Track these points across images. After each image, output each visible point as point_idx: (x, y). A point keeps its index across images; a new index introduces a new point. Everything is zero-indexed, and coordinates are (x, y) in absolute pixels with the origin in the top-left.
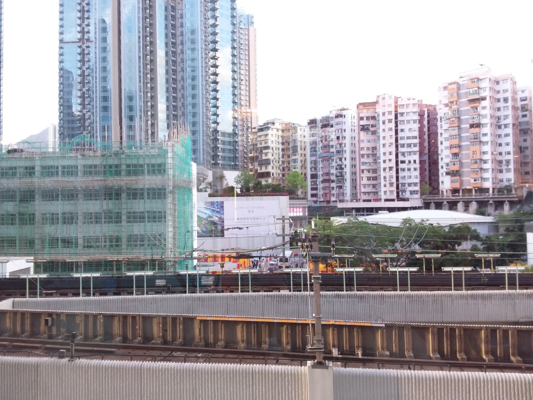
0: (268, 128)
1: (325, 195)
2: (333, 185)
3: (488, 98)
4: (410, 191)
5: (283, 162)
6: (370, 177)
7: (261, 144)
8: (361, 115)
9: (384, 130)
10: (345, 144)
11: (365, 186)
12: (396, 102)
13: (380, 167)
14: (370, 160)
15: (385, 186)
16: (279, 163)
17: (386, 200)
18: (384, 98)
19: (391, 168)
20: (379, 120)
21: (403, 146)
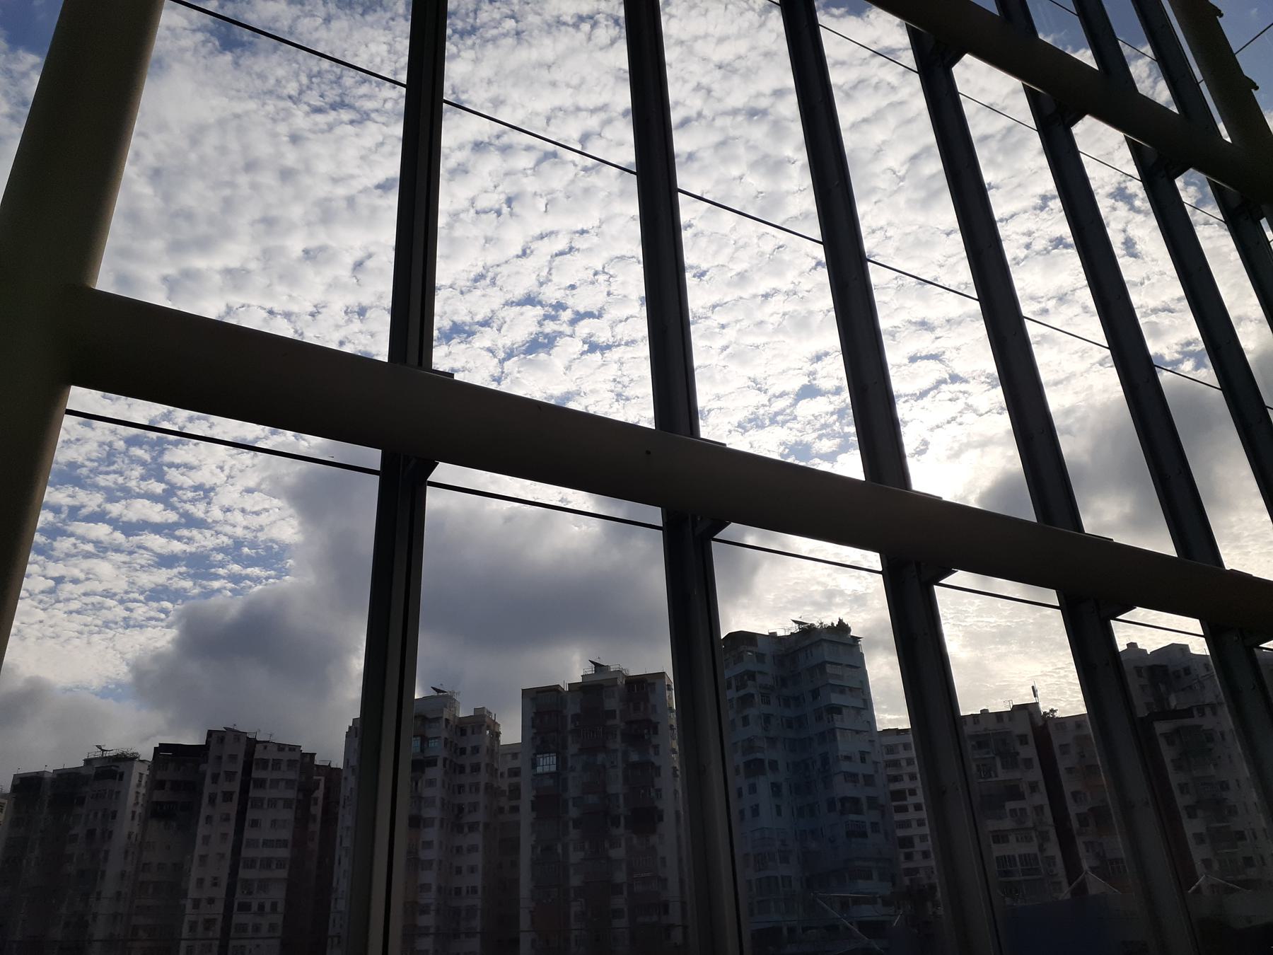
3: (440, 763)
21: (251, 864)
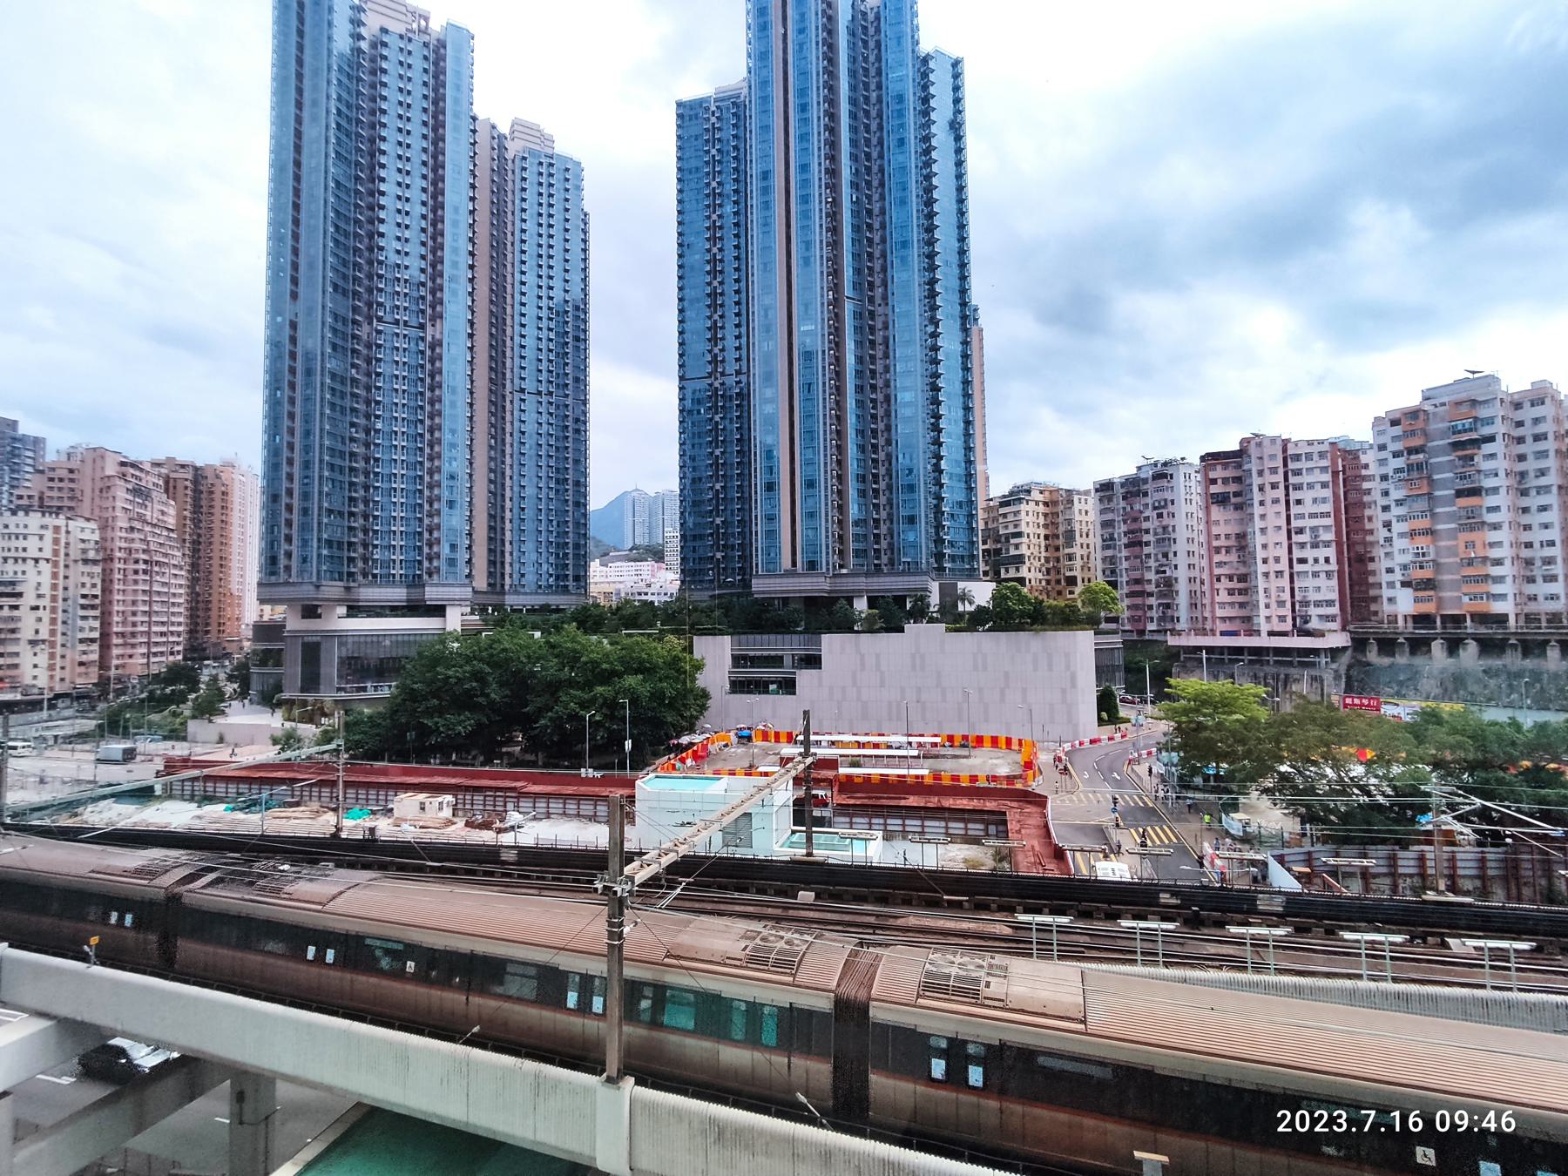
1: (1132, 619)
2: (1152, 601)
4: (1320, 616)
5: (1047, 560)
7: (1006, 527)
8: (1212, 475)
9: (1262, 503)
11: (1222, 605)
12: (1285, 450)
13: (1256, 572)
14: (1233, 557)
15: (1267, 606)
17: (1271, 634)
18: (1259, 445)
19: (1279, 573)
20: (1251, 485)
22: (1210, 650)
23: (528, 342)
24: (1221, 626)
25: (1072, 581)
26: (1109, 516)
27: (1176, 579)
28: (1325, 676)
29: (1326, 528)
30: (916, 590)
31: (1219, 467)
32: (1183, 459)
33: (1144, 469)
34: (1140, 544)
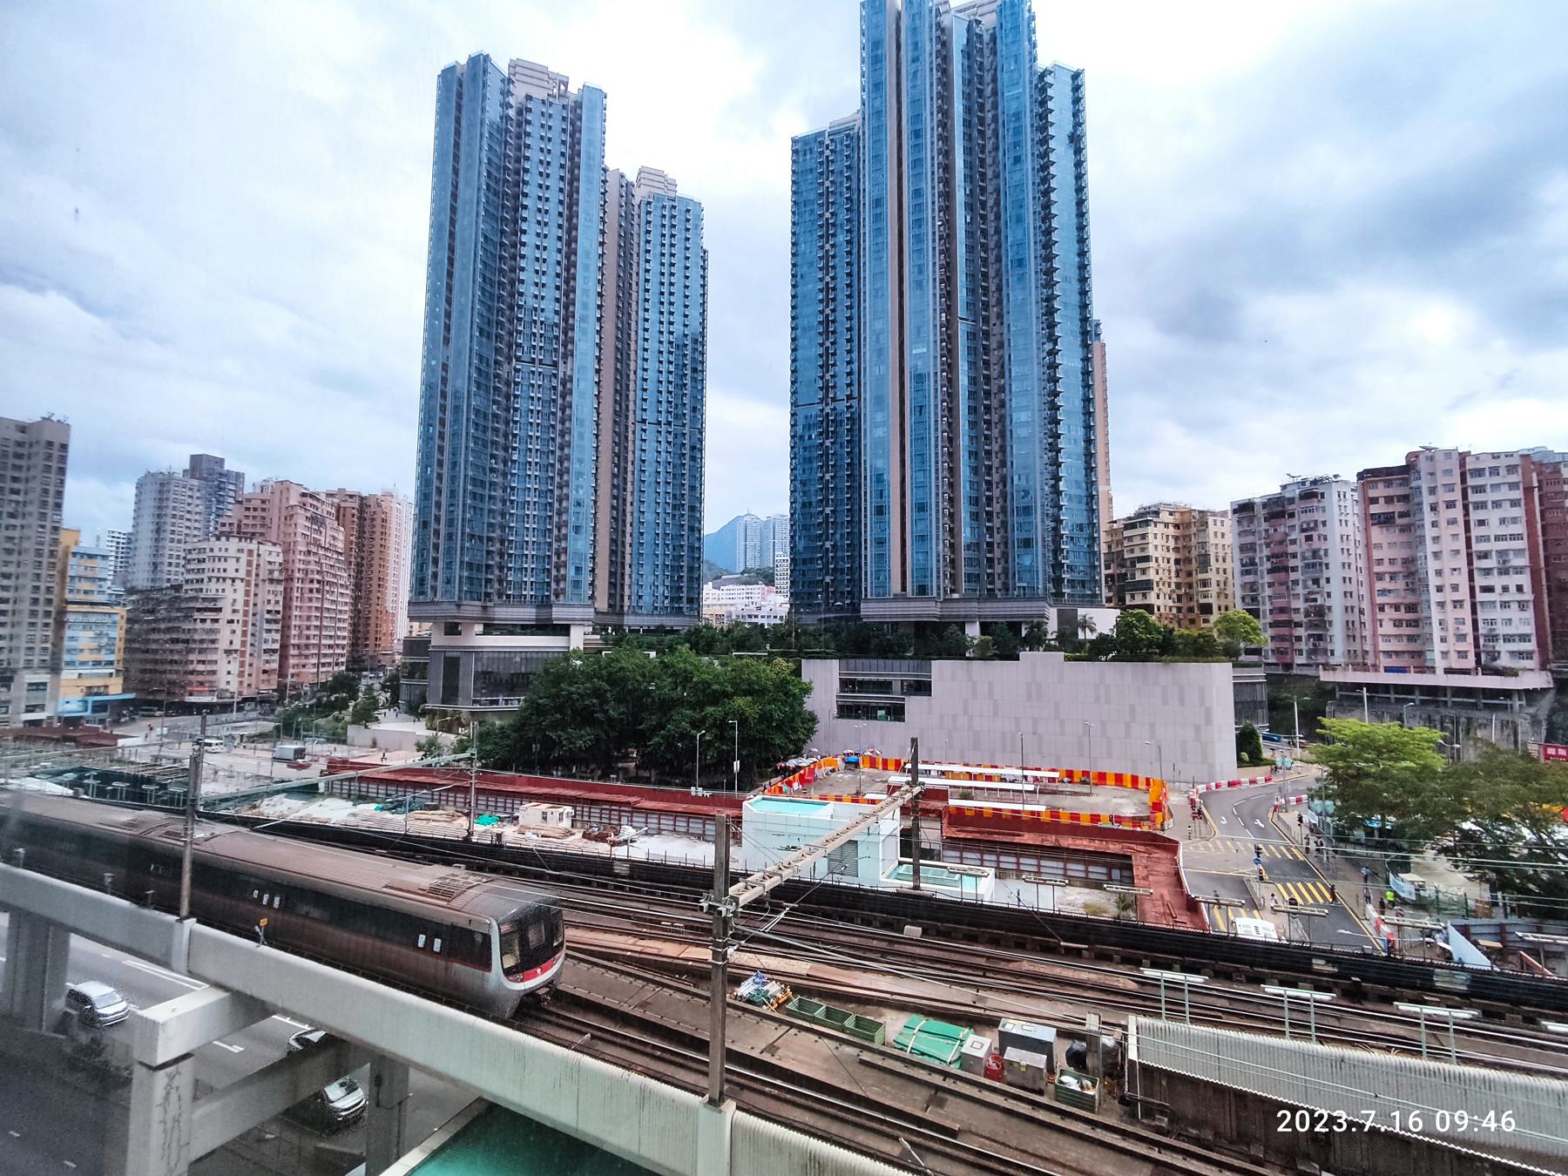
0: (1147, 523)
1: (1276, 651)
2: (1301, 632)
4: (1512, 653)
5: (1178, 586)
6: (1400, 621)
7: (1132, 551)
8: (1372, 493)
10: (1326, 551)
11: (1387, 637)
12: (1462, 464)
14: (1400, 584)
16: (1169, 586)
17: (1449, 671)
18: (1432, 458)
19: (1457, 604)
20: (1420, 504)
22: (1372, 687)
23: (651, 315)
24: (1384, 661)
25: (1207, 609)
26: (1249, 539)
27: (1330, 608)
28: (1519, 721)
29: (1518, 552)
30: (1032, 616)
31: (1381, 485)
32: (1335, 476)
33: (1289, 488)
34: (1286, 569)
